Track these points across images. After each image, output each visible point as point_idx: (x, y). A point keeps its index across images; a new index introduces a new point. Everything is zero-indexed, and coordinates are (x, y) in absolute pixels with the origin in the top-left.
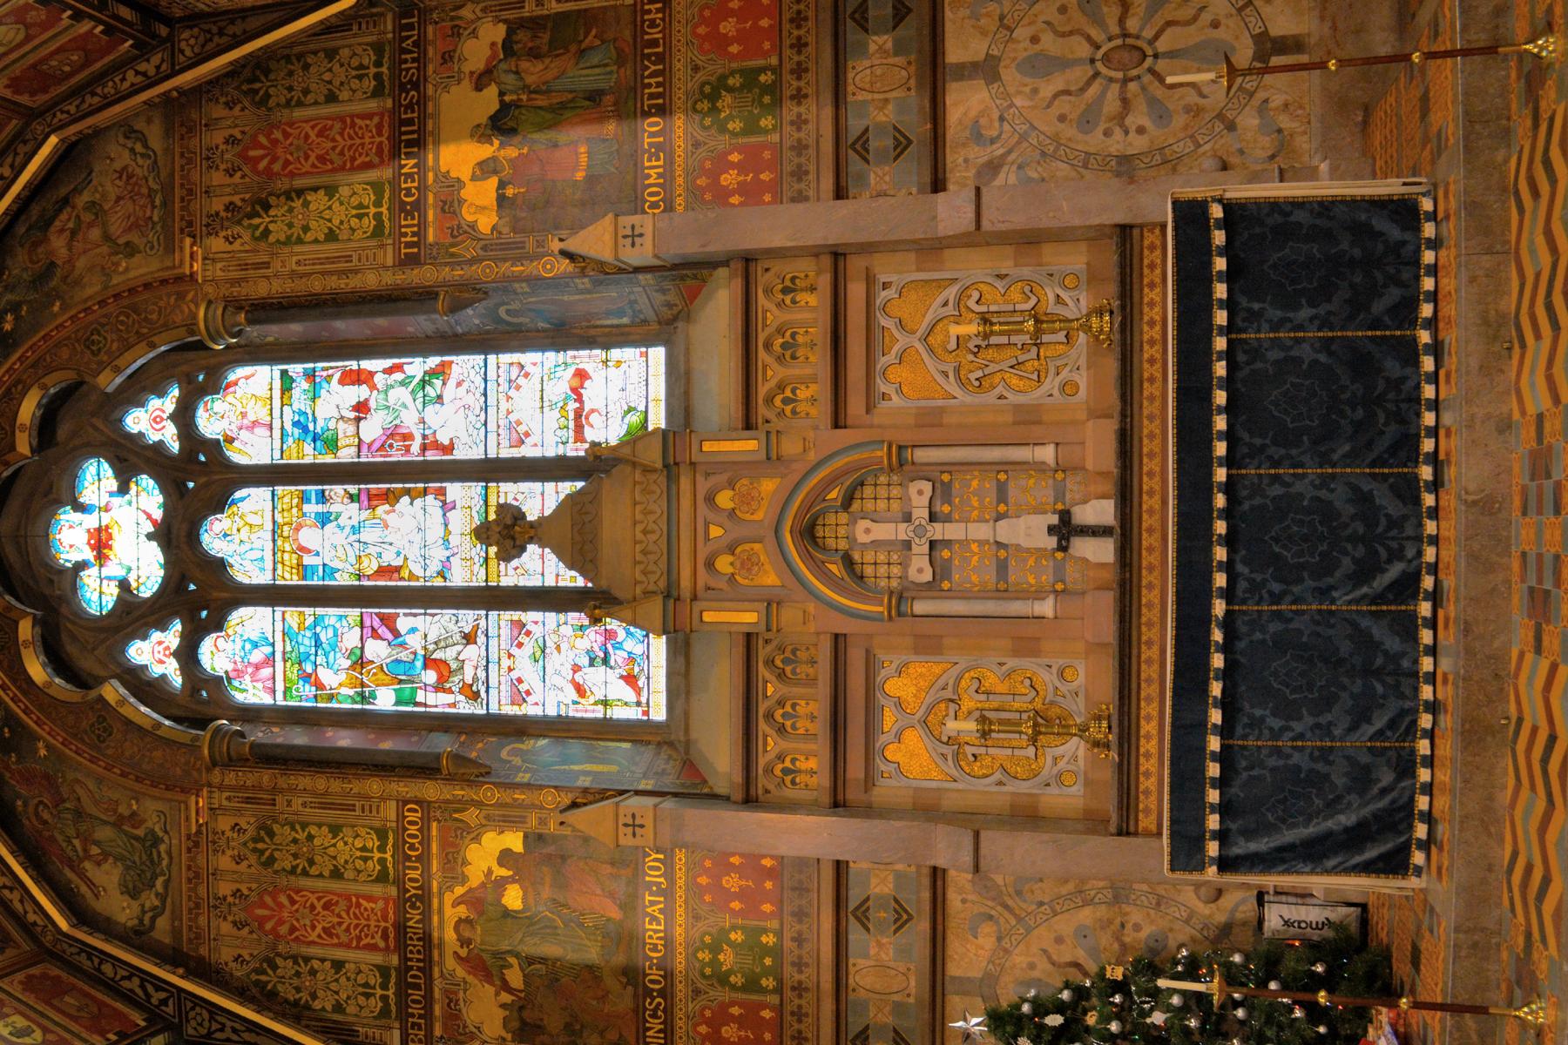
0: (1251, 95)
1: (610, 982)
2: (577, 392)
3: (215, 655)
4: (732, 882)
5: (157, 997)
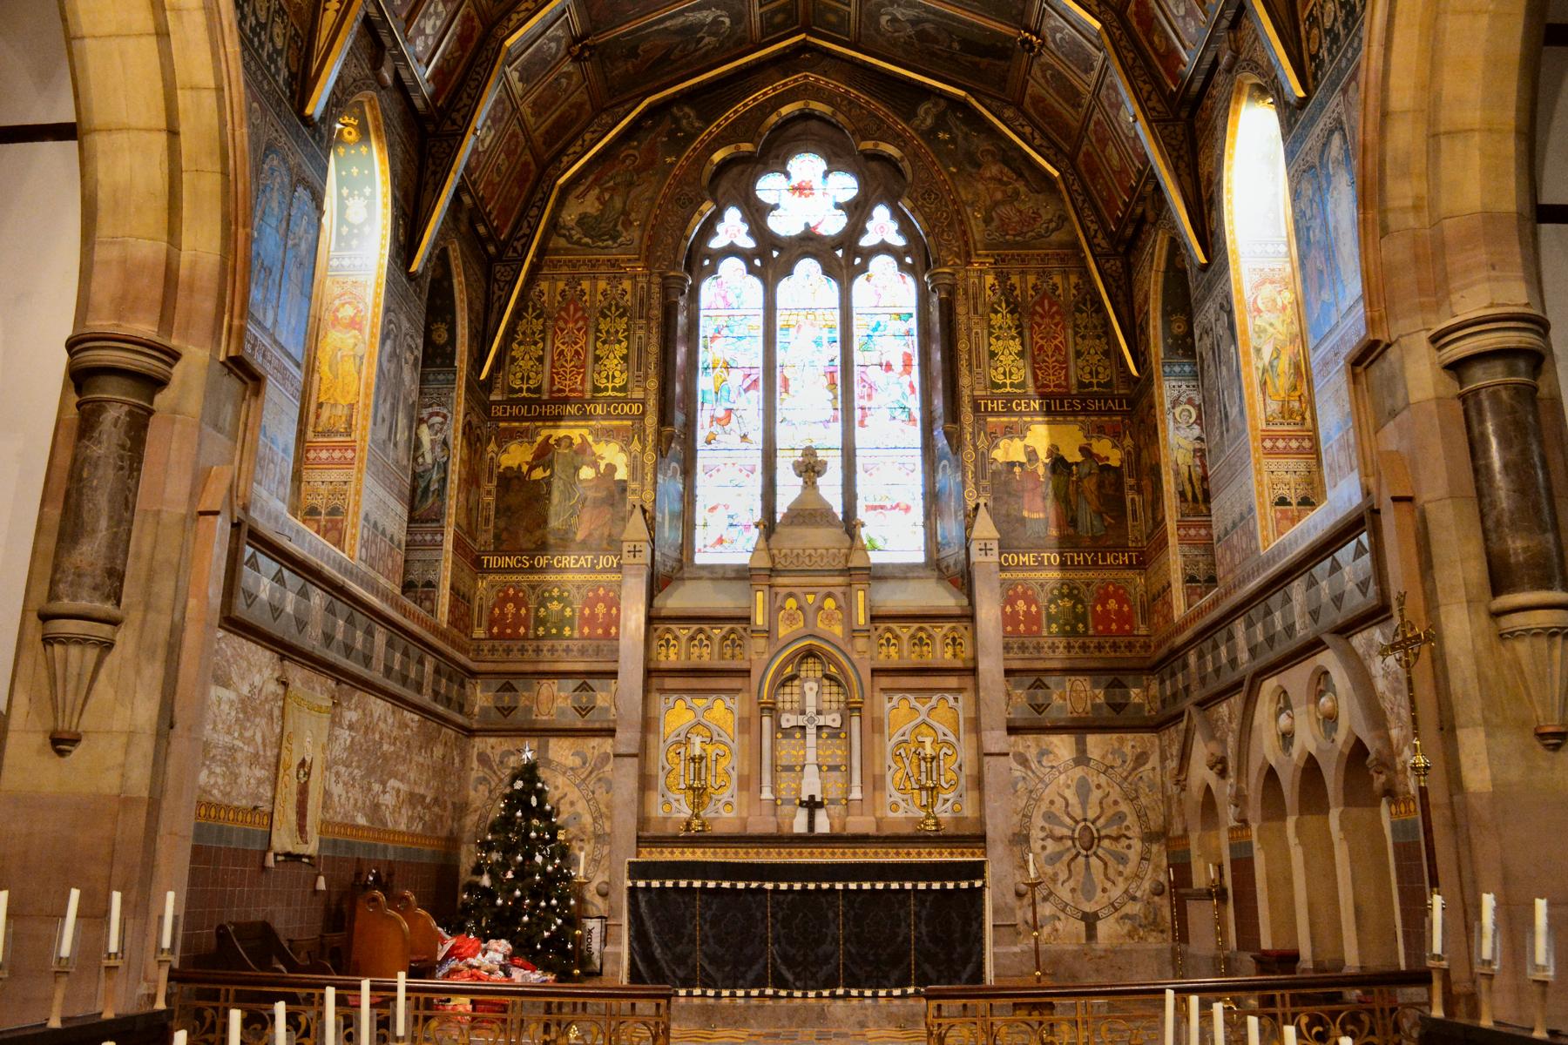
0: (1063, 911)
1: (538, 533)
3: (732, 268)
4: (601, 609)
5: (518, 245)
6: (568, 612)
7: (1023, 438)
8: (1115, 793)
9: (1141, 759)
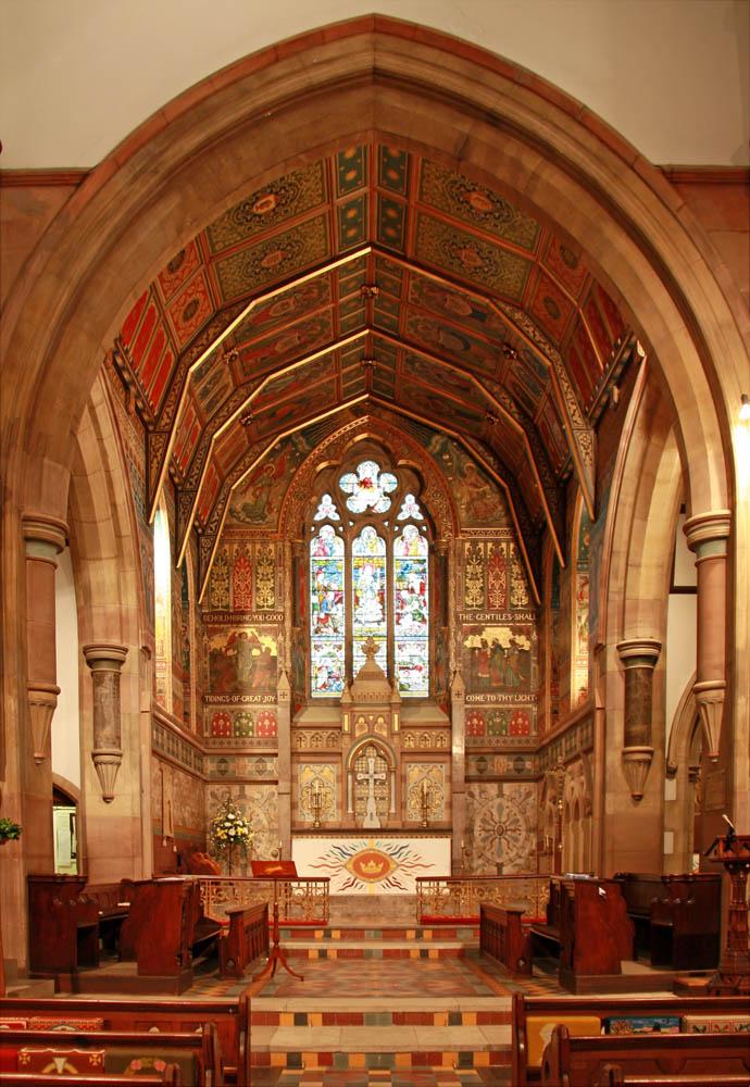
1: (233, 684)
2: (415, 668)
3: (327, 532)
6: (251, 724)
7: (480, 634)
8: (515, 810)
9: (528, 794)
